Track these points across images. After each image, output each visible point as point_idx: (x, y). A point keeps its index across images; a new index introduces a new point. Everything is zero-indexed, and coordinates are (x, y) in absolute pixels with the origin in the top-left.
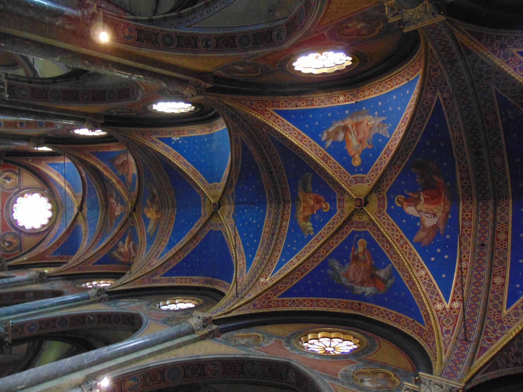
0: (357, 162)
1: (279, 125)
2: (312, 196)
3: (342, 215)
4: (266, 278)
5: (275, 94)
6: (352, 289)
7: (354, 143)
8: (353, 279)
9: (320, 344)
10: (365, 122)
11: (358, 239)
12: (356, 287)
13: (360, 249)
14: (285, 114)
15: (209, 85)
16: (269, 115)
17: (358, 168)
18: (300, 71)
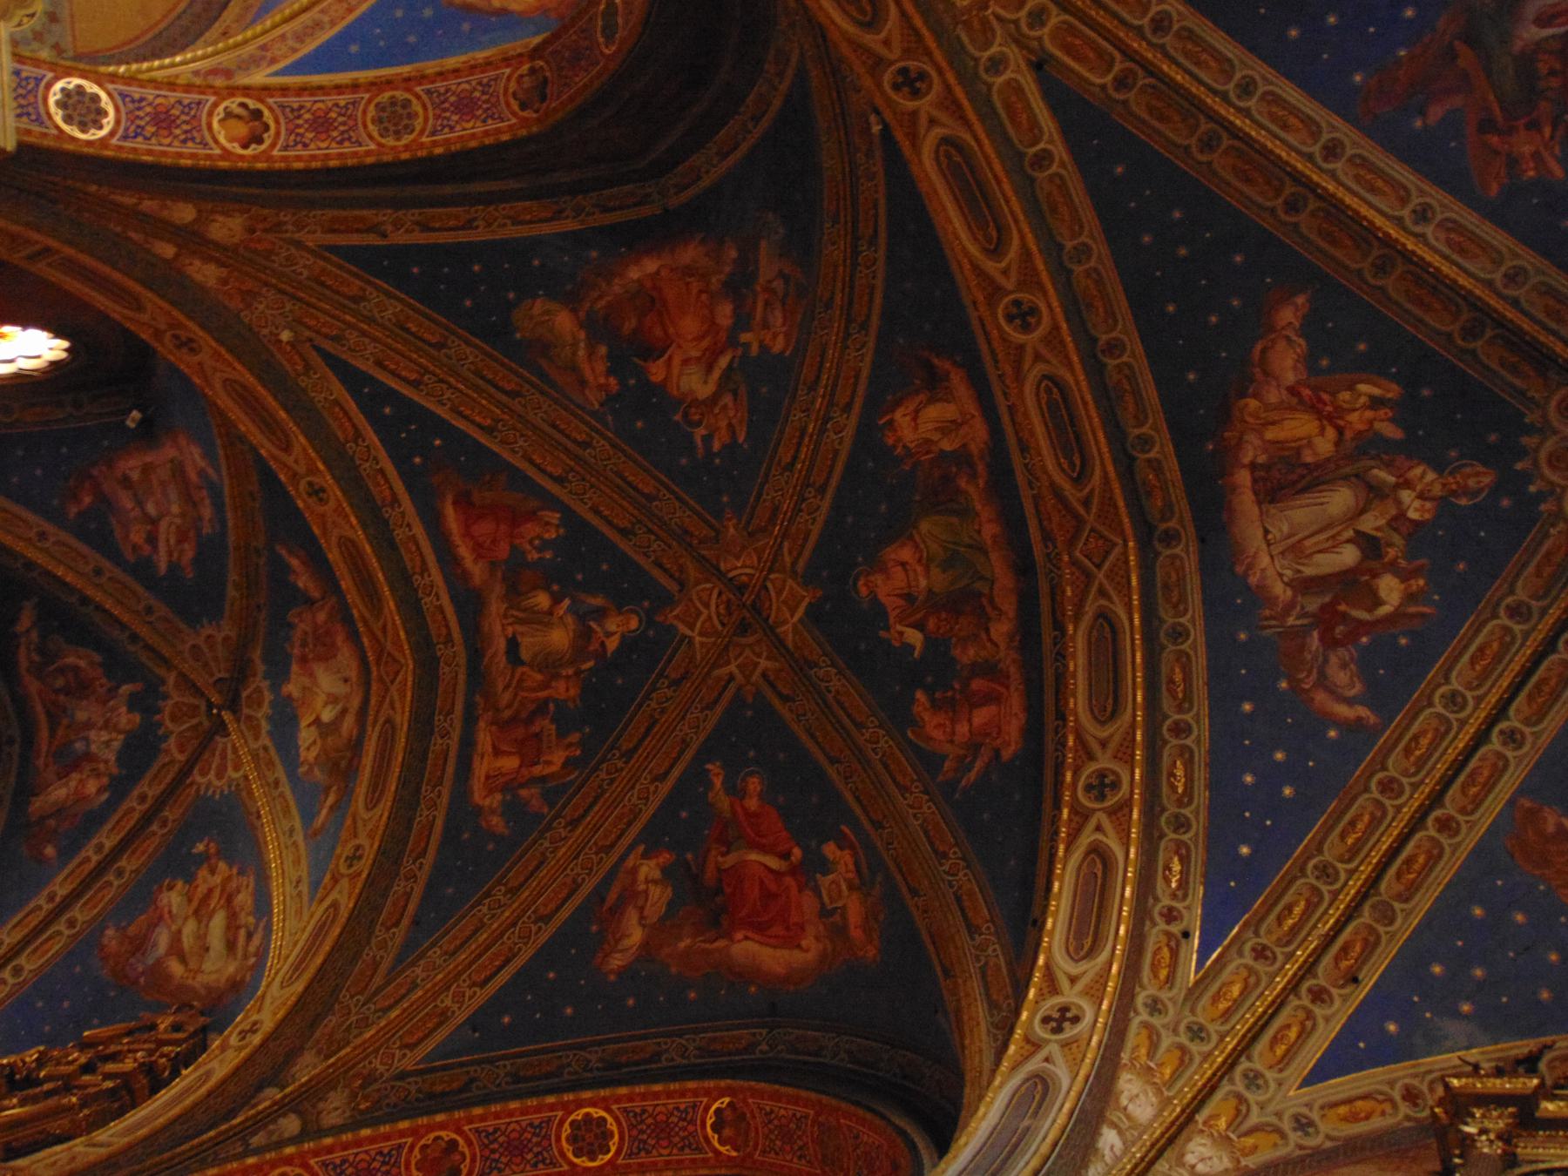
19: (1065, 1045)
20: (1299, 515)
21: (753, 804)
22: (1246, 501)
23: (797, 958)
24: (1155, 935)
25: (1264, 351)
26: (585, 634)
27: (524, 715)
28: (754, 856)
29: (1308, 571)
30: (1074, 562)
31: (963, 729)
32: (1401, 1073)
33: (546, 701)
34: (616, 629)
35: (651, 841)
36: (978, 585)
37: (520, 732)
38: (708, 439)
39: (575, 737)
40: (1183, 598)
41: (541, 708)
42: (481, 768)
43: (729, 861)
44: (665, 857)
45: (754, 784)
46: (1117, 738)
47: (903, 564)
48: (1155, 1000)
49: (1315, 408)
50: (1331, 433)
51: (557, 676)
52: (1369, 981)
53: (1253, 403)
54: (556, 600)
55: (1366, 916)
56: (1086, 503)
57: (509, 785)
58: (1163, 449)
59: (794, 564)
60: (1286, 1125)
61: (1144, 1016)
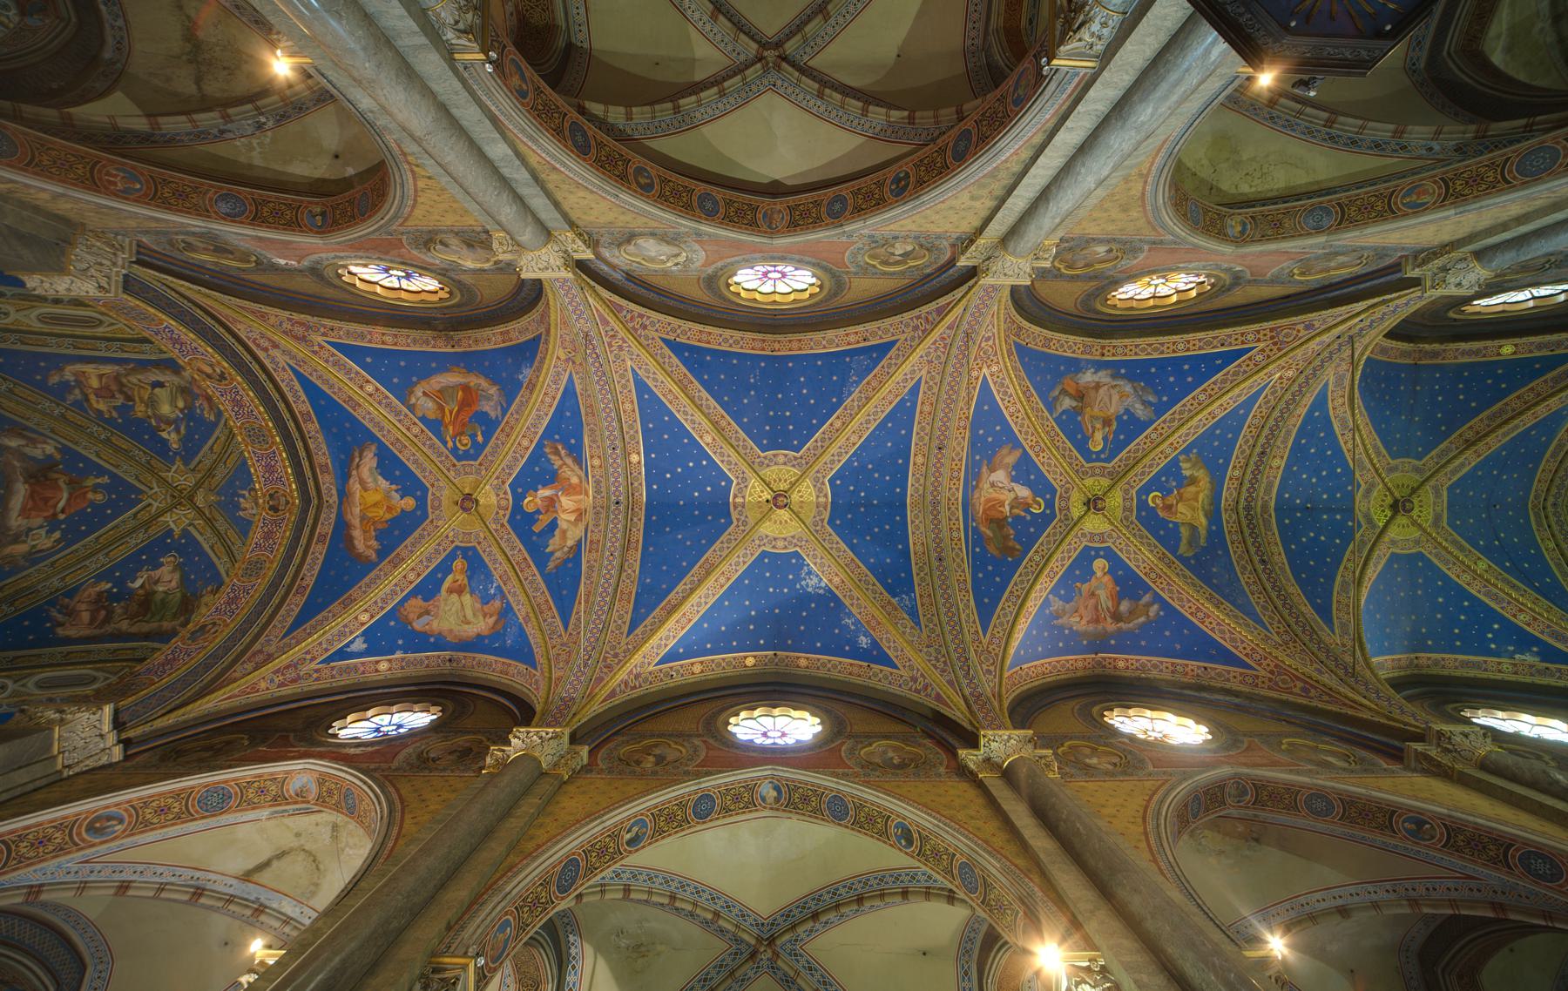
0: (1100, 565)
1: (1243, 642)
2: (1178, 519)
3: (1127, 487)
4: (1281, 378)
5: (1250, 697)
6: (1114, 377)
7: (1103, 595)
8: (1112, 391)
9: (1173, 285)
10: (1084, 622)
11: (1102, 451)
12: (1108, 380)
13: (1099, 436)
14: (1228, 658)
15: (1419, 747)
16: (1265, 663)
17: (1097, 556)
18: (1198, 722)
23: (14, 514)
26: (169, 422)
27: (125, 389)
28: (65, 495)
31: (84, 607)
33: (133, 400)
34: (171, 437)
35: (64, 450)
37: (114, 387)
38: (243, 496)
39: (115, 414)
41: (129, 398)
42: (89, 369)
44: (58, 456)
45: (99, 497)
51: (147, 406)
54: (182, 411)
57: (80, 383)
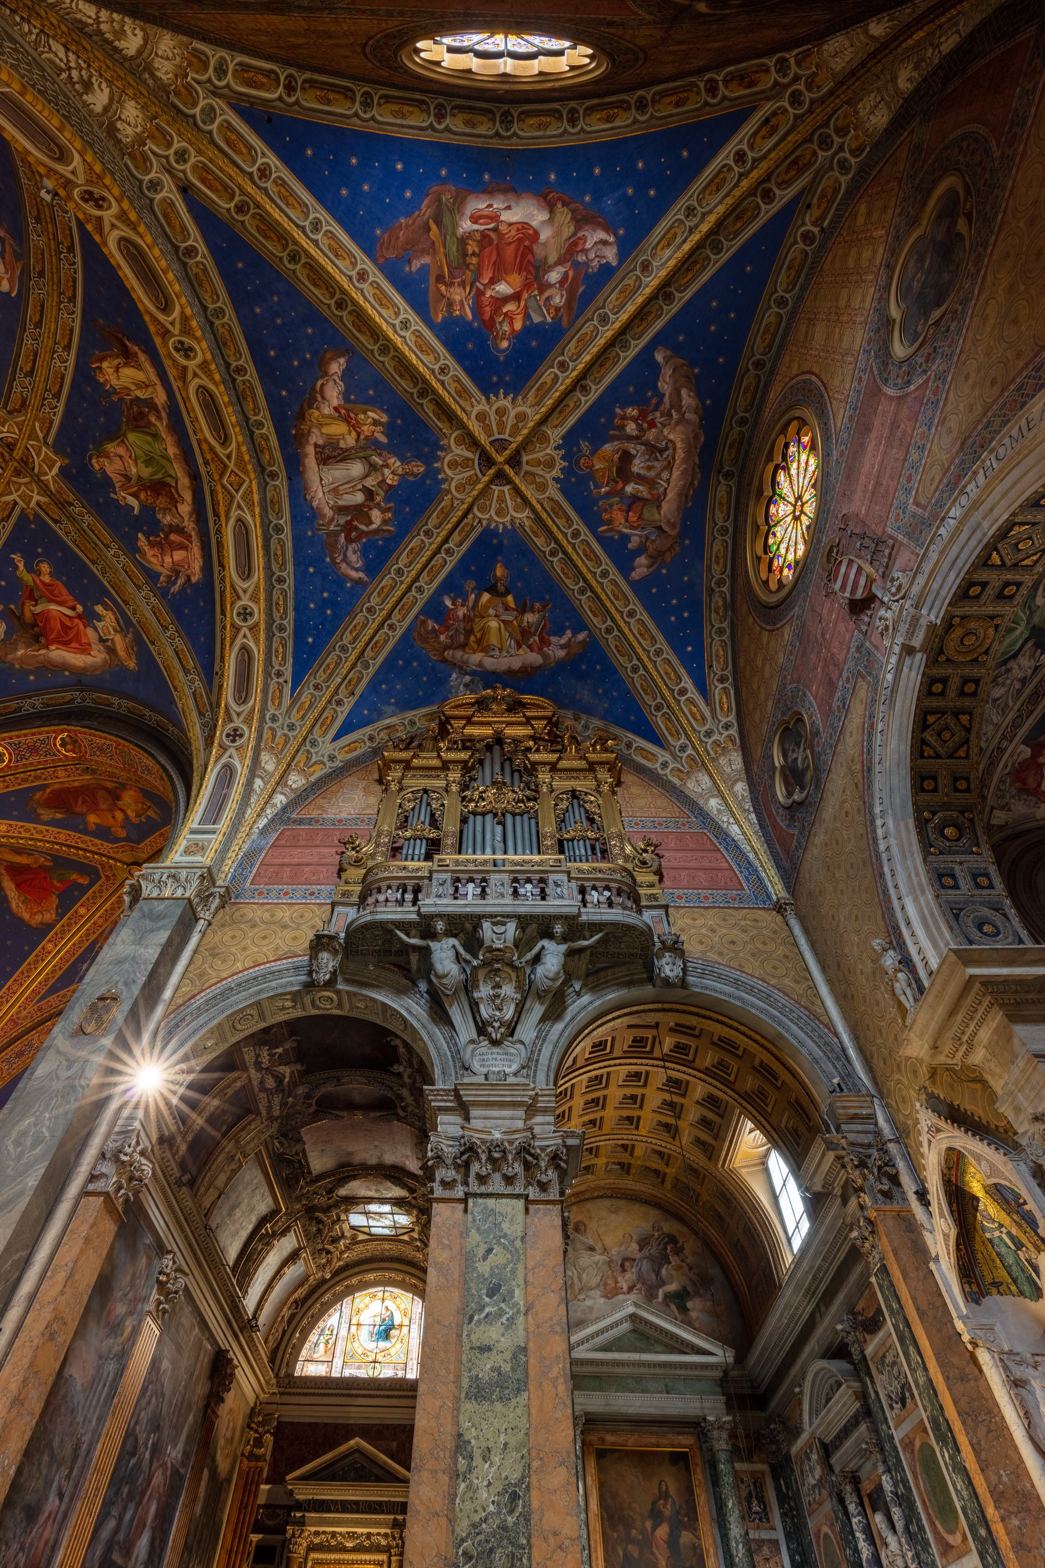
19: (237, 749)
20: (336, 473)
21: (47, 579)
22: (311, 461)
24: (273, 686)
25: (322, 385)
28: (53, 607)
29: (341, 503)
30: (223, 487)
31: (168, 560)
32: (368, 730)
36: (168, 480)
40: (280, 510)
43: (38, 609)
45: (45, 568)
46: (251, 590)
47: (120, 457)
48: (274, 715)
49: (347, 420)
50: (354, 434)
52: (358, 692)
53: (316, 413)
55: (359, 667)
56: (229, 457)
58: (268, 430)
59: (46, 437)
60: (325, 760)
61: (270, 724)
